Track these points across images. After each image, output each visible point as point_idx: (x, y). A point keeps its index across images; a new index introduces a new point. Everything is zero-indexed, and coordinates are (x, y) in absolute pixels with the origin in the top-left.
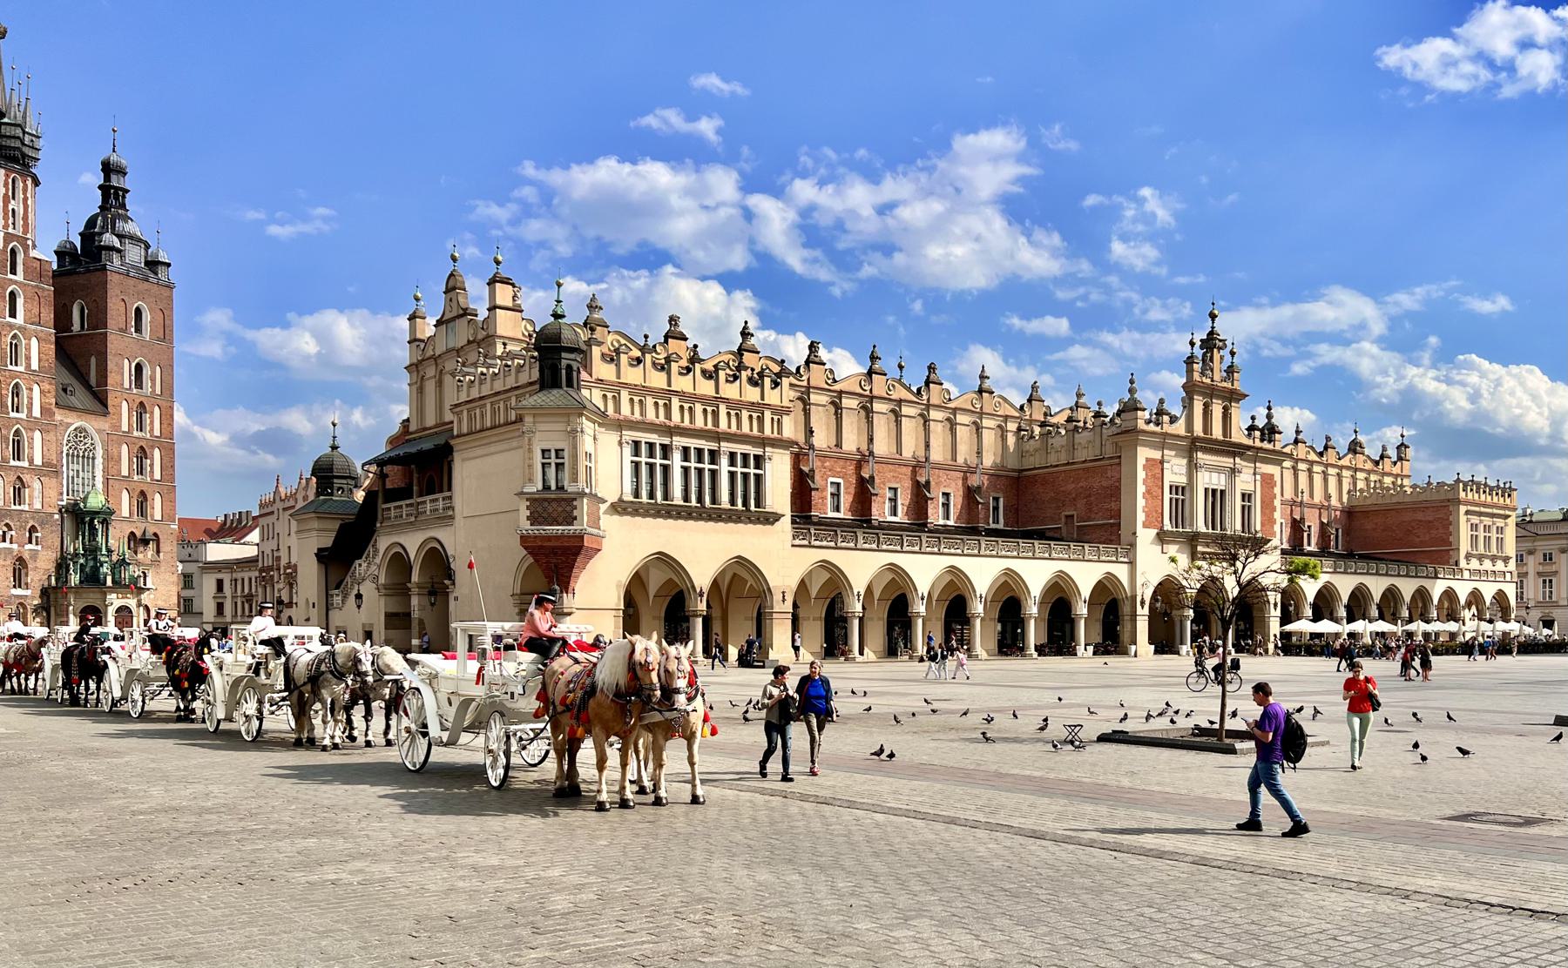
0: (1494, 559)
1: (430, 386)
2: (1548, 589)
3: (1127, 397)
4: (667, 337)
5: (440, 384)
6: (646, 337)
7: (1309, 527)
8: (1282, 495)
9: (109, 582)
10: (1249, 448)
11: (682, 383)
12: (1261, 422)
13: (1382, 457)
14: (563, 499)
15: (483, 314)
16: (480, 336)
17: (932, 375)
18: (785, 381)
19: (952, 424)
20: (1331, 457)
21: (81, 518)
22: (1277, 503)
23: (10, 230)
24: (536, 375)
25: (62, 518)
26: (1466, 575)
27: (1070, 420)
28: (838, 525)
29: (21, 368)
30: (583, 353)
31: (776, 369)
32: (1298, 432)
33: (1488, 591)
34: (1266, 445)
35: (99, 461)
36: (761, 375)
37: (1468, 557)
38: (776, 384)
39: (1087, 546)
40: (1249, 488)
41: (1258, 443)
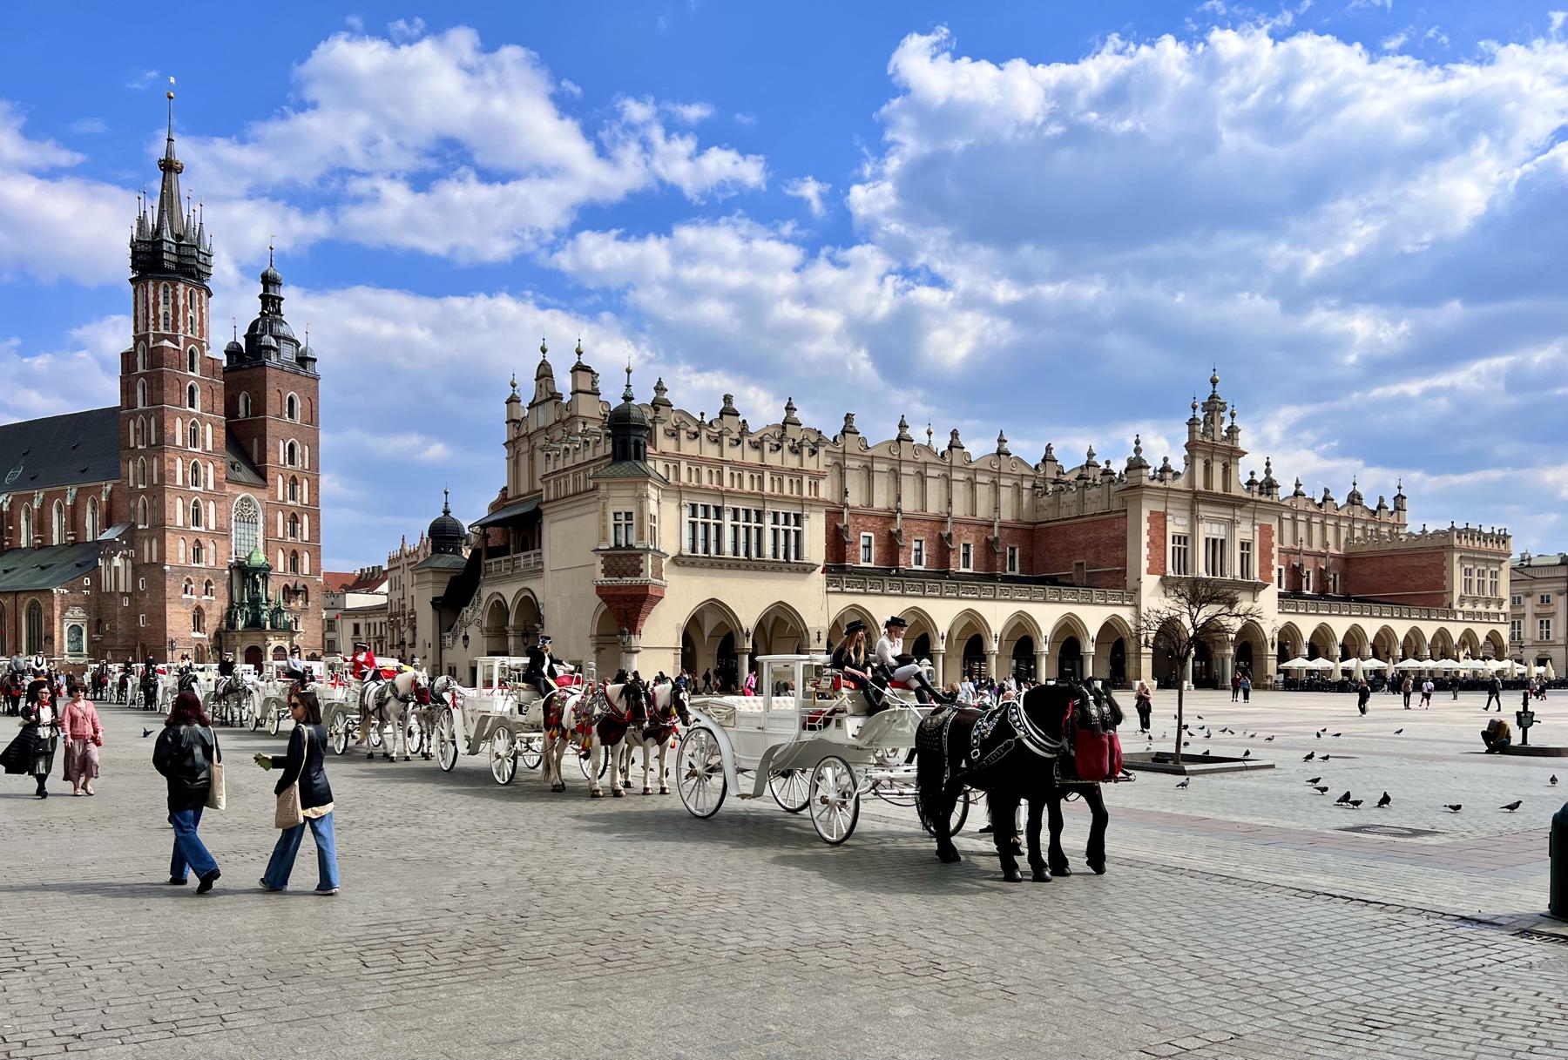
0: (1488, 602)
1: (524, 459)
2: (1545, 630)
4: (722, 413)
5: (532, 457)
6: (702, 414)
7: (1308, 572)
8: (1281, 541)
10: (1248, 500)
11: (733, 454)
12: (1260, 477)
14: (632, 555)
15: (567, 398)
16: (565, 417)
17: (955, 440)
18: (822, 451)
19: (972, 484)
20: (1329, 509)
22: (1275, 551)
23: (189, 335)
24: (609, 449)
25: (231, 573)
26: (1460, 616)
27: (1080, 478)
29: (199, 450)
31: (814, 439)
32: (1298, 485)
33: (1482, 632)
37: (1462, 600)
38: (814, 452)
39: (1094, 591)
40: (1249, 537)
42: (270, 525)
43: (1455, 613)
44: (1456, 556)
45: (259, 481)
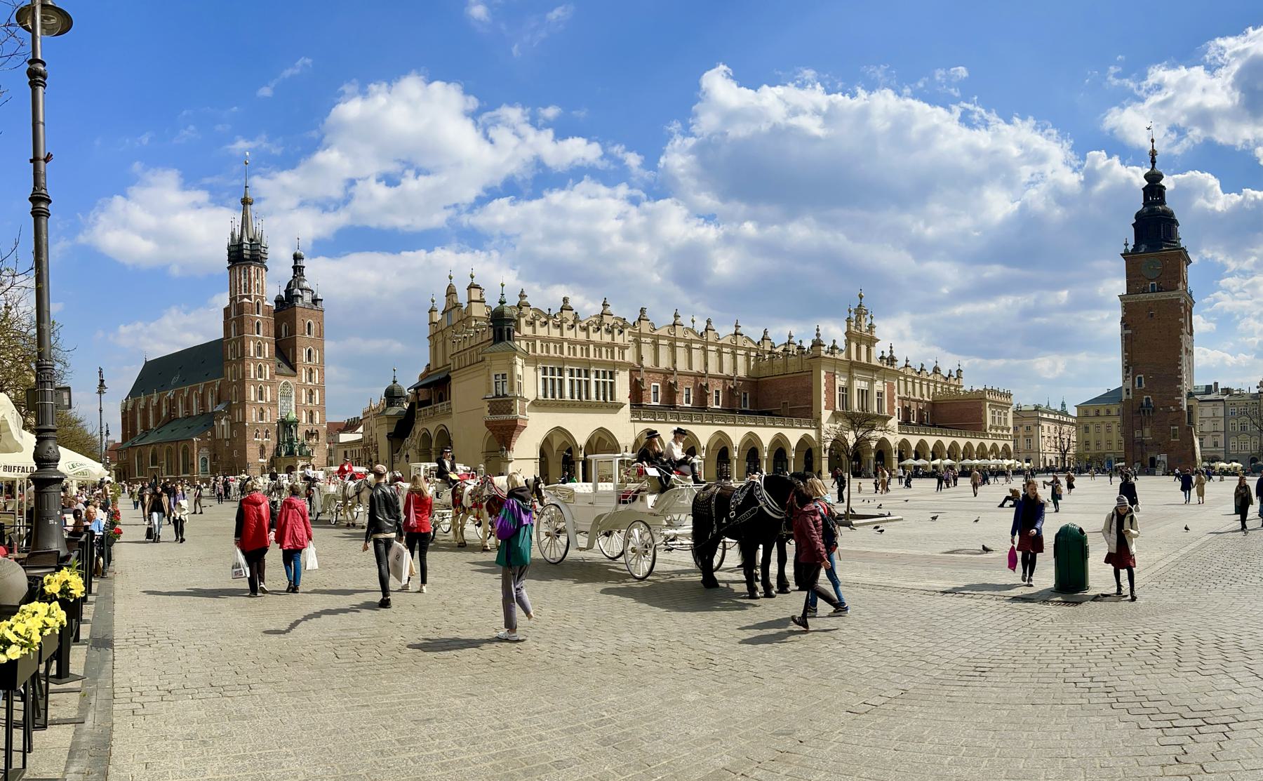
1: (440, 346)
3: (816, 338)
4: (562, 309)
5: (444, 344)
6: (549, 310)
8: (899, 393)
9: (298, 454)
11: (569, 334)
12: (887, 355)
13: (949, 376)
15: (465, 306)
16: (464, 317)
18: (626, 331)
19: (720, 353)
20: (924, 375)
21: (286, 425)
22: (896, 398)
26: (990, 436)
28: (656, 409)
30: (518, 323)
31: (621, 324)
32: (907, 361)
33: (1000, 444)
34: (889, 367)
35: (293, 397)
36: (613, 327)
37: (991, 428)
38: (621, 332)
39: (794, 419)
41: (885, 366)
42: (298, 396)
43: (987, 434)
44: (988, 404)
45: (291, 372)
